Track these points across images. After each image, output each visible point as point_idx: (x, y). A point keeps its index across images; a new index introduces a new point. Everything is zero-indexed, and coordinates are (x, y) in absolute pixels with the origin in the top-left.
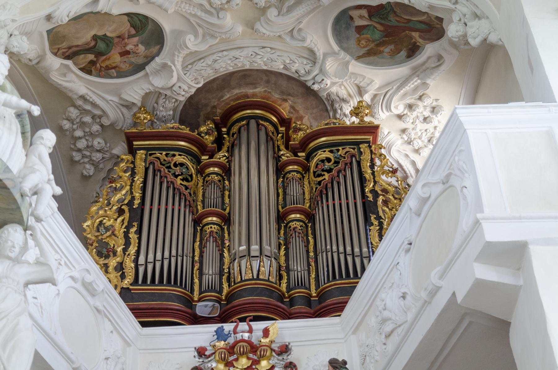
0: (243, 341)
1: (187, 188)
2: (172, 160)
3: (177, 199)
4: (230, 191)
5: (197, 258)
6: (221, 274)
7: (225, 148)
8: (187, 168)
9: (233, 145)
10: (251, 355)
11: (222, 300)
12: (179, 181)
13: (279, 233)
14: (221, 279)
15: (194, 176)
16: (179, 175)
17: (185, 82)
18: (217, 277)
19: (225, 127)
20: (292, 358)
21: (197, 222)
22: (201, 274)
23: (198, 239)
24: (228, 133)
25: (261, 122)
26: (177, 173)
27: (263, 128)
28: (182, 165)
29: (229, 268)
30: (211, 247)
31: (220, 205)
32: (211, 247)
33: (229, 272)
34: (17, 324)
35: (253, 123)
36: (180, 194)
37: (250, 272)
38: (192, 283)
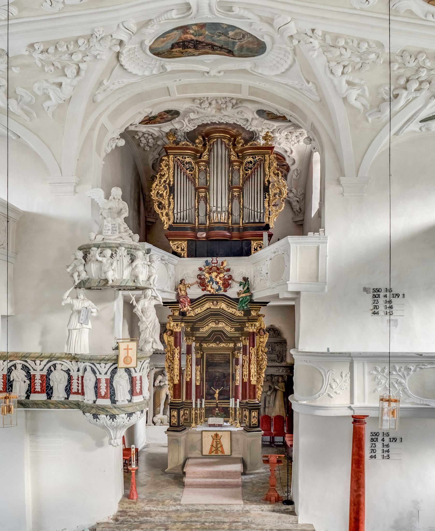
0: (214, 266)
1: (191, 175)
2: (185, 161)
3: (188, 180)
4: (209, 174)
5: (196, 207)
6: (206, 215)
7: (207, 150)
8: (191, 164)
9: (210, 151)
10: (217, 271)
11: (206, 227)
12: (188, 172)
13: (229, 196)
15: (194, 167)
16: (188, 169)
17: (189, 127)
18: (205, 217)
19: (207, 137)
20: (230, 273)
21: (197, 189)
22: (198, 215)
23: (197, 198)
24: (209, 142)
25: (223, 140)
26: (187, 168)
27: (224, 143)
28: (190, 163)
29: (209, 213)
30: (202, 203)
31: (205, 185)
33: (209, 214)
35: (219, 140)
36: (189, 178)
37: (217, 218)
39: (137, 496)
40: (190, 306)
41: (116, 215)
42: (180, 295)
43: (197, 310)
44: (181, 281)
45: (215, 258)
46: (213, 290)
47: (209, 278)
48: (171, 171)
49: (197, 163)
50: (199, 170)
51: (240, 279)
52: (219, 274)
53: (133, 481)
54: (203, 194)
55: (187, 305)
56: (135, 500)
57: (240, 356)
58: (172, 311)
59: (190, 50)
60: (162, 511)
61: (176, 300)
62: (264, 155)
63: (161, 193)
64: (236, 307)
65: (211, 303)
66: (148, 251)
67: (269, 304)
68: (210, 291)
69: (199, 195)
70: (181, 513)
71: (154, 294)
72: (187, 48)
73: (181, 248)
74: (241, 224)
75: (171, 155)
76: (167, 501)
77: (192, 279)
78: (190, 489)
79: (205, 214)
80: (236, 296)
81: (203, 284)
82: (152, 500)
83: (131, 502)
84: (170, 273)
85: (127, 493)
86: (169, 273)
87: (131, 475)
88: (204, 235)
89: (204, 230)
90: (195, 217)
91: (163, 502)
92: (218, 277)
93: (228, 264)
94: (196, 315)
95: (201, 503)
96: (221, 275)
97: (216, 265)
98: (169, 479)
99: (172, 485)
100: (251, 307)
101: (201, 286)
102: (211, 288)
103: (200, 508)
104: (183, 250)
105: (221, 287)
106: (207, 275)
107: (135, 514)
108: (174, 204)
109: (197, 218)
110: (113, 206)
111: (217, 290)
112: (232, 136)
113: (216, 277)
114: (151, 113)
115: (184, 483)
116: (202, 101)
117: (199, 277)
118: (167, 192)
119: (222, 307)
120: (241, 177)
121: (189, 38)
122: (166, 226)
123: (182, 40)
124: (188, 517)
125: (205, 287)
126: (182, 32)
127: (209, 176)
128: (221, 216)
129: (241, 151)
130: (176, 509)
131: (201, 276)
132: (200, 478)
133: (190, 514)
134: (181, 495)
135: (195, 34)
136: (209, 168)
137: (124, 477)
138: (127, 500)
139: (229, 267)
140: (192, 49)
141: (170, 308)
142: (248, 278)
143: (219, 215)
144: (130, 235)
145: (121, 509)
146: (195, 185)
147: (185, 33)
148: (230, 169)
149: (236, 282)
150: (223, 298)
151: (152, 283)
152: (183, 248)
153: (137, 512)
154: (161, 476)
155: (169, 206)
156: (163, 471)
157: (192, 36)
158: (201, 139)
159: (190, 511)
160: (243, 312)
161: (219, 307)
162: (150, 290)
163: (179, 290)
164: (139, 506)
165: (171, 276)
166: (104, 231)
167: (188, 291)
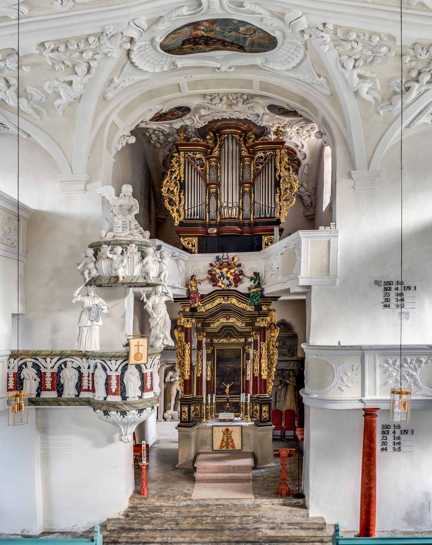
0: (225, 262)
1: (202, 171)
4: (220, 169)
5: (207, 203)
9: (221, 146)
12: (199, 168)
14: (217, 213)
17: (200, 124)
18: (216, 213)
19: (218, 133)
20: (241, 268)
21: (207, 185)
23: (207, 194)
24: (219, 137)
28: (200, 159)
30: (213, 199)
32: (213, 199)
34: (166, 320)
35: (230, 135)
38: (206, 215)
39: (148, 492)
40: (201, 301)
41: (126, 212)
42: (191, 291)
43: (208, 305)
44: (192, 277)
45: (225, 254)
46: (224, 286)
47: (220, 274)
48: (182, 167)
49: (208, 159)
50: (210, 166)
51: (251, 274)
52: (230, 269)
53: (144, 477)
54: (214, 190)
55: (197, 301)
56: (146, 496)
57: (251, 351)
58: (182, 307)
59: (201, 46)
60: (173, 507)
61: (186, 296)
62: (274, 150)
63: (171, 189)
64: (247, 302)
65: (222, 299)
66: (159, 248)
67: (280, 298)
68: (221, 287)
69: (209, 191)
70: (191, 508)
71: (165, 290)
72: (198, 44)
73: (192, 244)
74: (252, 219)
75: (182, 151)
76: (178, 497)
77: (202, 275)
78: (201, 484)
79: (216, 210)
80: (247, 291)
81: (213, 280)
82: (162, 496)
83: (141, 497)
84: (181, 269)
85: (137, 489)
86: (180, 269)
87: (142, 471)
88: (215, 231)
89: (215, 226)
90: (206, 213)
91: (174, 497)
92: (229, 273)
93: (239, 260)
94: (206, 311)
95: (212, 498)
96: (232, 271)
97: (226, 260)
98: (179, 474)
99: (183, 480)
100: (261, 302)
101: (212, 282)
102: (222, 283)
103: (210, 503)
104: (193, 246)
105: (232, 282)
106: (218, 271)
107: (146, 510)
108: (185, 200)
109: (207, 214)
110: (124, 203)
111: (228, 286)
112: (243, 131)
113: (227, 273)
114: (162, 110)
115: (195, 478)
116: (213, 97)
117: (210, 272)
118: (177, 189)
119: (232, 303)
120: (252, 173)
121: (200, 35)
122: (176, 222)
123: (193, 36)
124: (199, 512)
125: (216, 282)
126: (193, 28)
127: (220, 171)
128: (232, 212)
129: (253, 146)
130: (187, 504)
131: (212, 271)
132: (211, 473)
133: (201, 509)
134: (192, 490)
135: (206, 31)
136: (220, 164)
137: (135, 473)
138: (138, 496)
139: (240, 262)
140: (203, 46)
141: (180, 304)
142: (259, 273)
143: (230, 211)
144: (141, 232)
145: (131, 505)
146: (205, 181)
147: (196, 29)
148: (241, 164)
149: (247, 277)
150: (234, 293)
151: (162, 279)
152: (193, 244)
153: (147, 508)
154: (172, 472)
155: (180, 203)
156: (174, 466)
157: (203, 32)
158: (212, 135)
159: (201, 506)
160: (253, 307)
161: (229, 303)
162: (160, 286)
163: (190, 286)
164: (149, 502)
165: (181, 272)
166: (115, 229)
167: (199, 287)
